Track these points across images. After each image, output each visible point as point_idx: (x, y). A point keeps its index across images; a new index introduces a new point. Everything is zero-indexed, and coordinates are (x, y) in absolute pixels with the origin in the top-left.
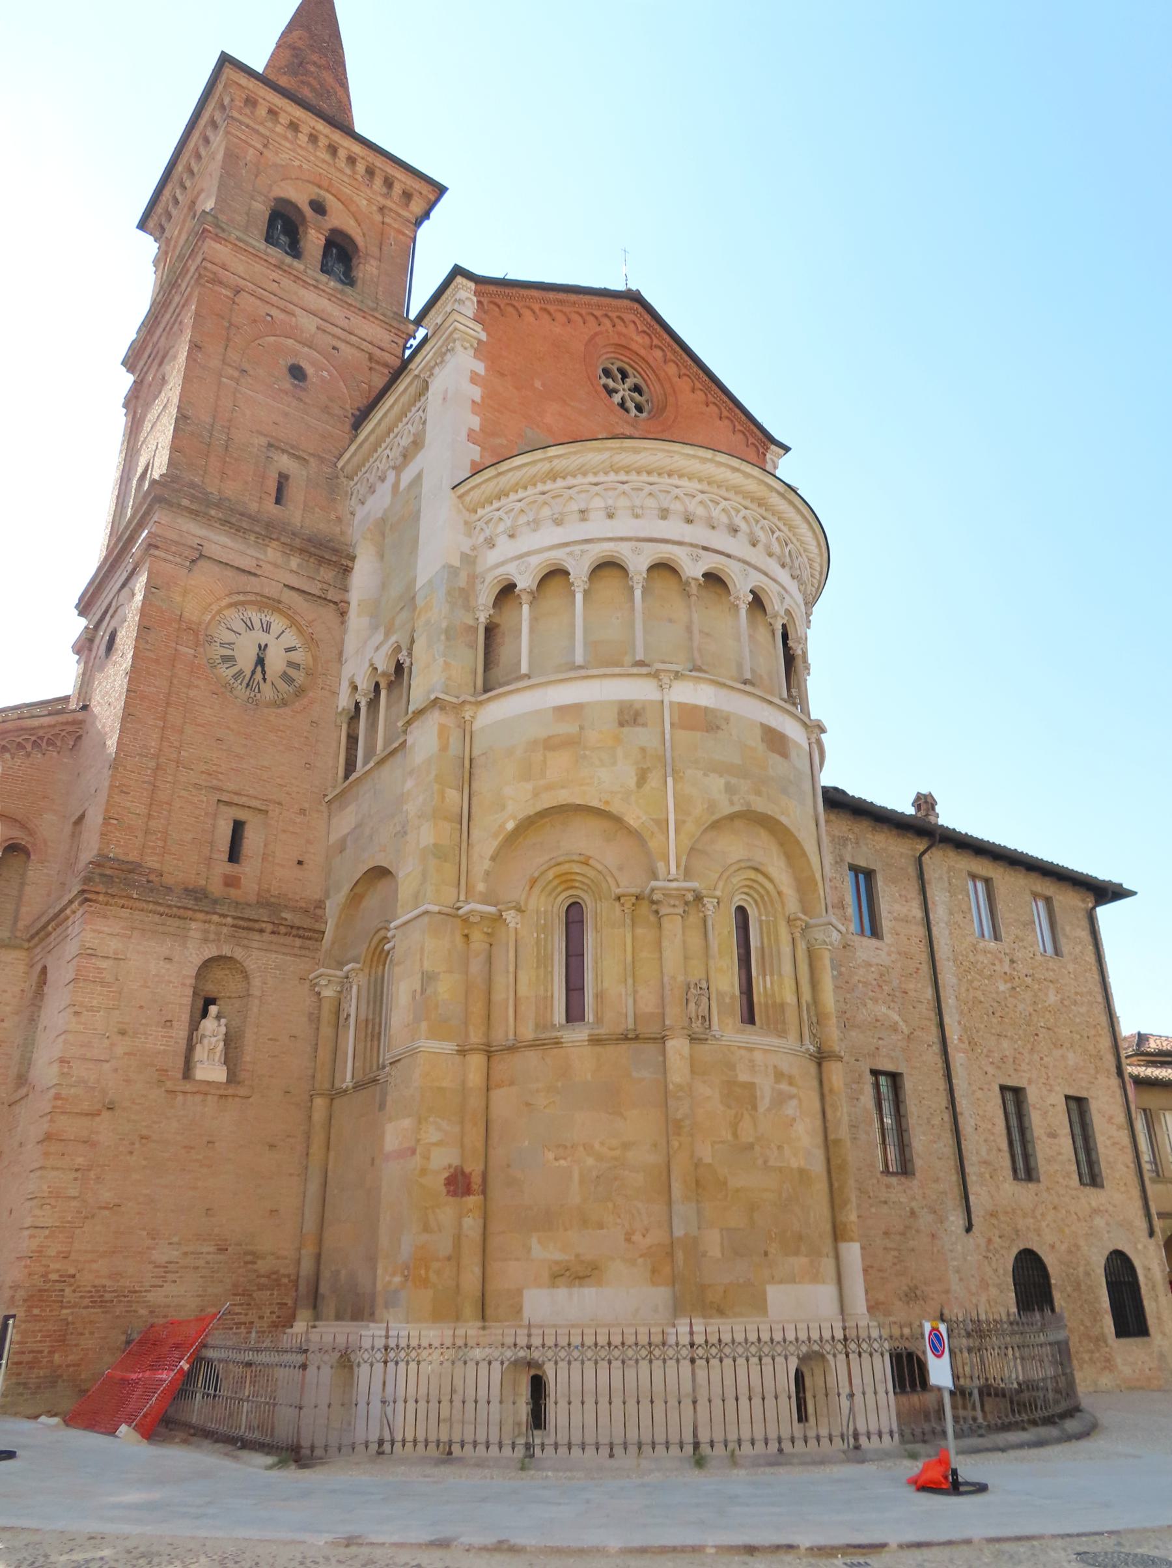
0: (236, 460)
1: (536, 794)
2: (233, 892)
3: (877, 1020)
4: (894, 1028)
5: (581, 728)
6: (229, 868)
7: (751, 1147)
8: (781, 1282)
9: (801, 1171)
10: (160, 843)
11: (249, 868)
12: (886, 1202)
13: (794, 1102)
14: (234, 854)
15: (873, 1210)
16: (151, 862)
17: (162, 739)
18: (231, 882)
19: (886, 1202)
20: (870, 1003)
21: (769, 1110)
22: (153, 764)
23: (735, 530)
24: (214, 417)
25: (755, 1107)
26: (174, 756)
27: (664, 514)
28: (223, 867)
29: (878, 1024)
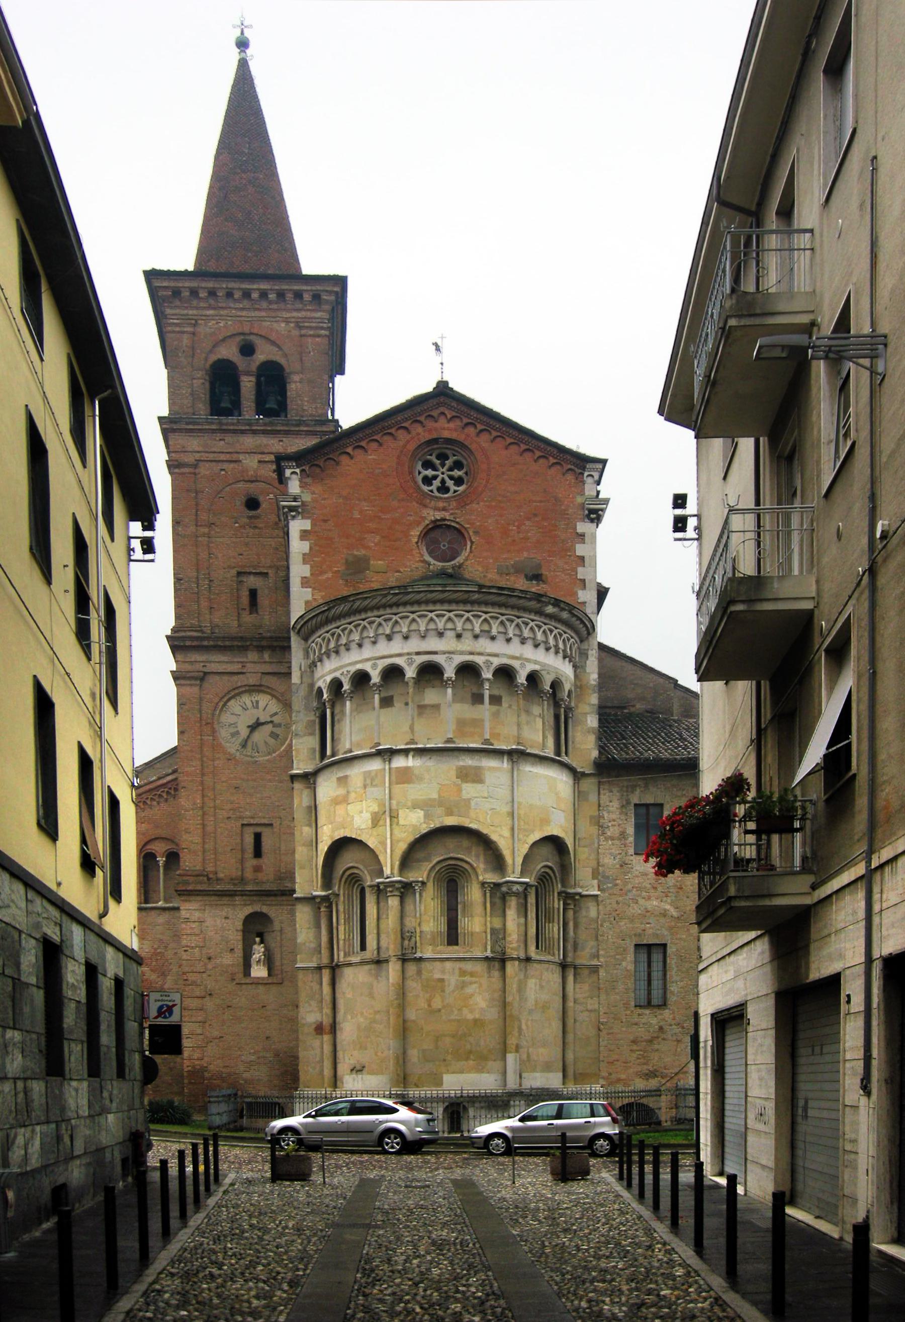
0: (218, 594)
1: (333, 831)
2: (260, 875)
3: (648, 912)
4: (664, 914)
5: (348, 792)
6: (255, 862)
7: (439, 1010)
8: (453, 1073)
9: (475, 1021)
10: (213, 856)
11: (267, 861)
12: (636, 1024)
13: (474, 986)
14: (258, 852)
15: (624, 1029)
16: (210, 868)
17: (203, 796)
18: (257, 869)
19: (636, 1024)
20: (641, 901)
21: (453, 991)
22: (200, 813)
23: (441, 635)
24: (198, 571)
25: (443, 991)
26: (212, 805)
27: (389, 638)
28: (251, 862)
29: (648, 914)
